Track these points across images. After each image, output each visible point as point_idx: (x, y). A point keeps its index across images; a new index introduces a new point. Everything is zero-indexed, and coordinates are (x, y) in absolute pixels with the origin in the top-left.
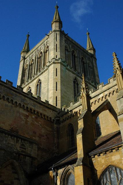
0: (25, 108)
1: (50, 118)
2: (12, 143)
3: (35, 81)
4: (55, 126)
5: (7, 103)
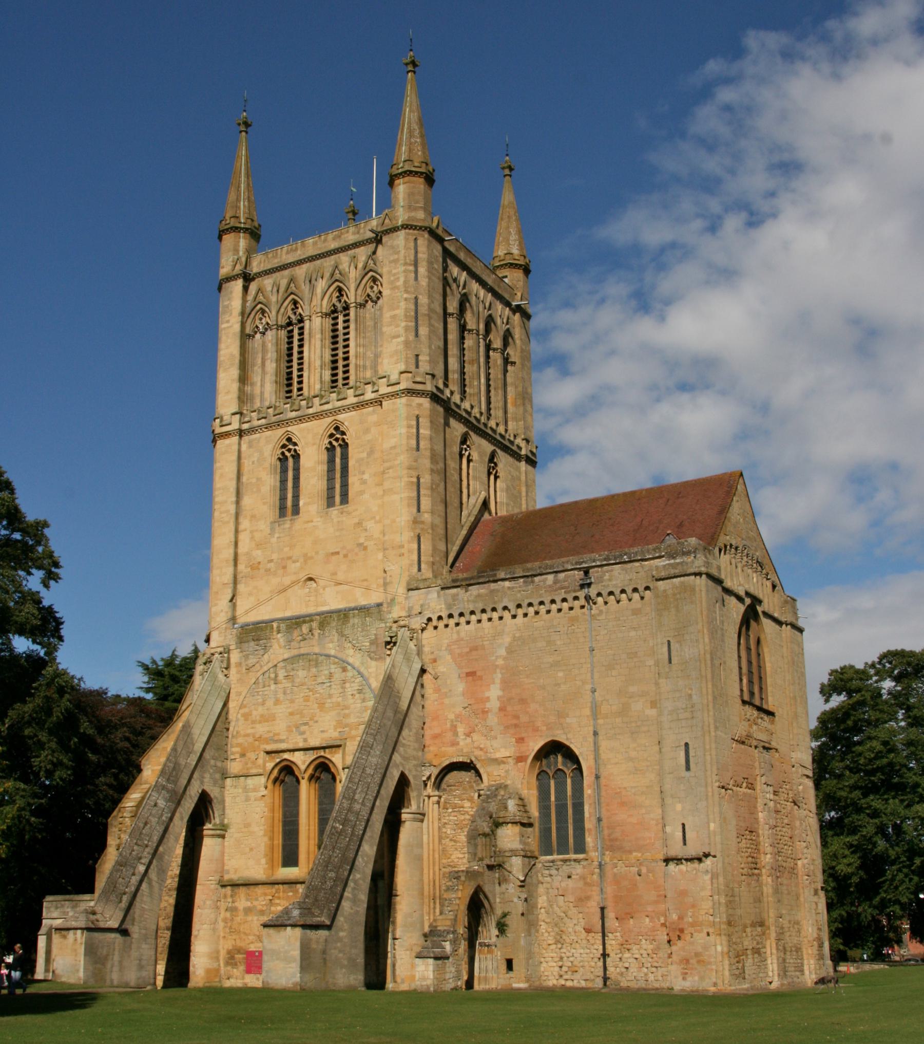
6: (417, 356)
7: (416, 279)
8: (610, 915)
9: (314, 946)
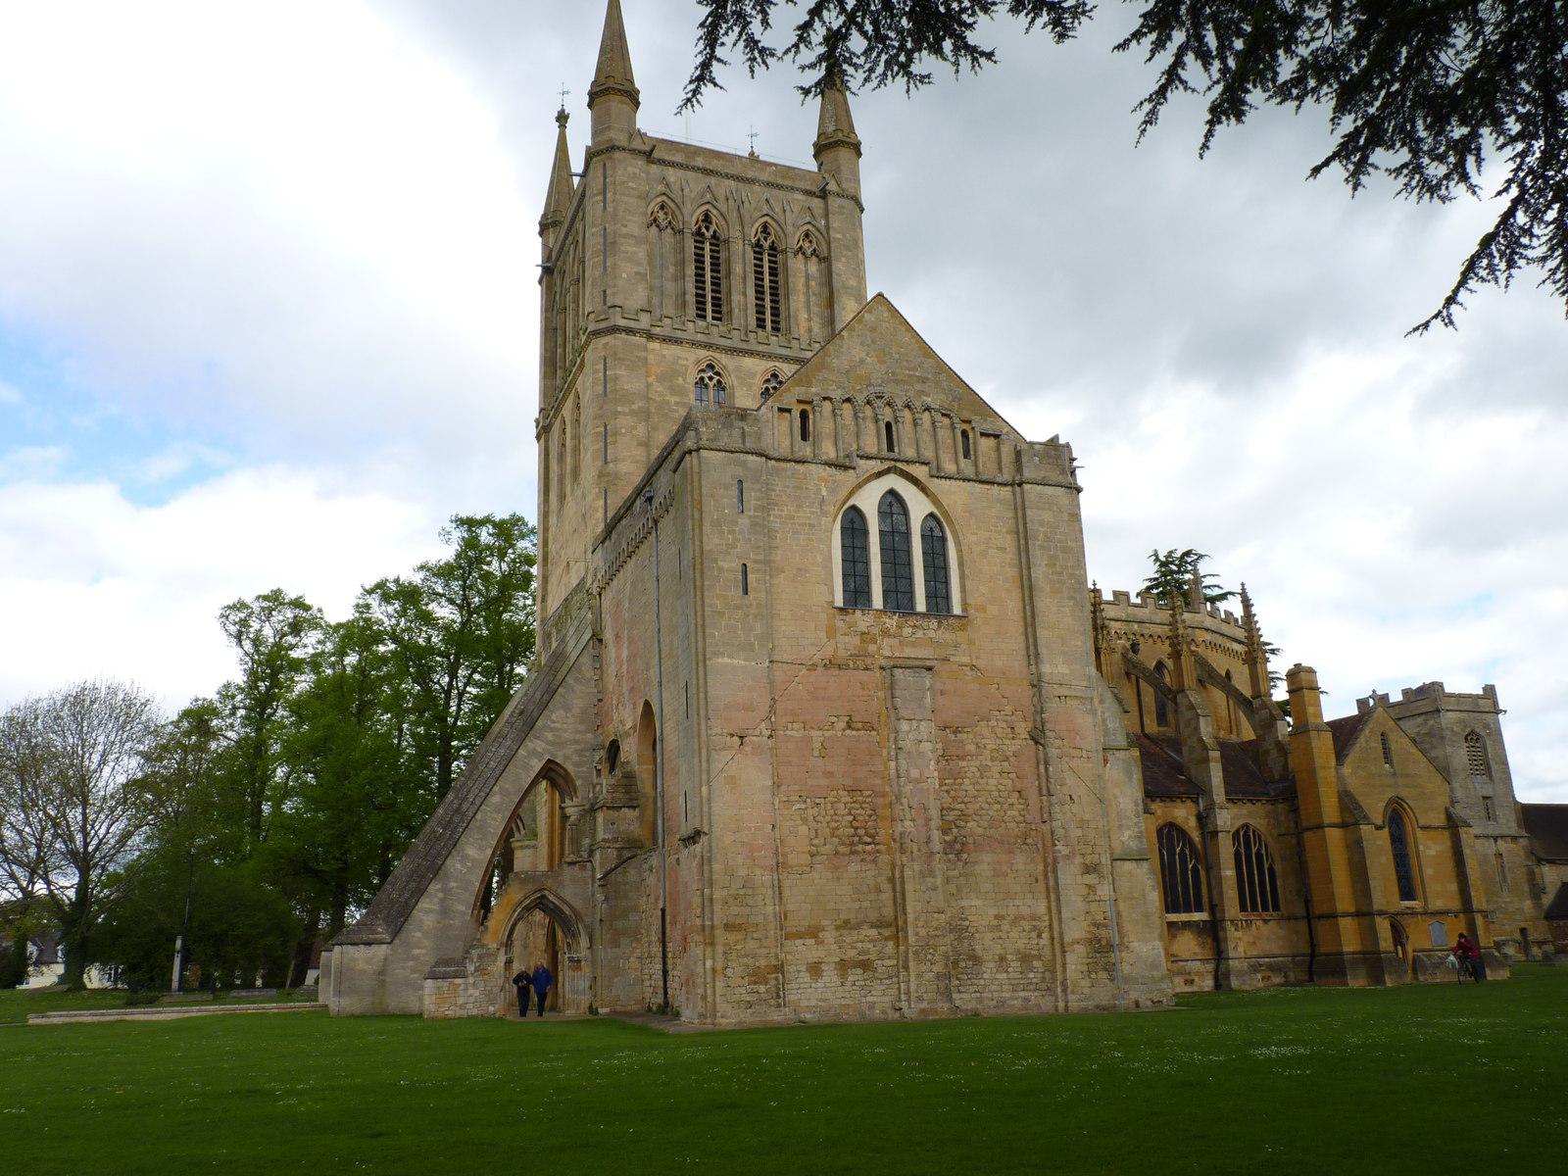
6: (605, 291)
7: (605, 208)
8: (668, 918)
9: (361, 965)
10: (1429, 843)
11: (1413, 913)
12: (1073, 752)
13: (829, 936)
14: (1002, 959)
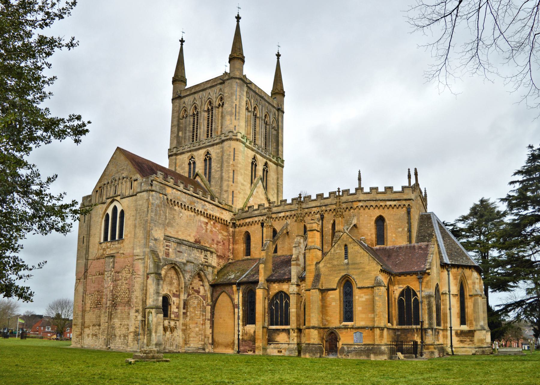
0: (205, 215)
1: (227, 221)
2: (198, 255)
3: (202, 152)
4: (231, 230)
5: (190, 213)
10: (362, 295)
11: (346, 328)
12: (138, 276)
13: (91, 328)
14: (120, 336)
